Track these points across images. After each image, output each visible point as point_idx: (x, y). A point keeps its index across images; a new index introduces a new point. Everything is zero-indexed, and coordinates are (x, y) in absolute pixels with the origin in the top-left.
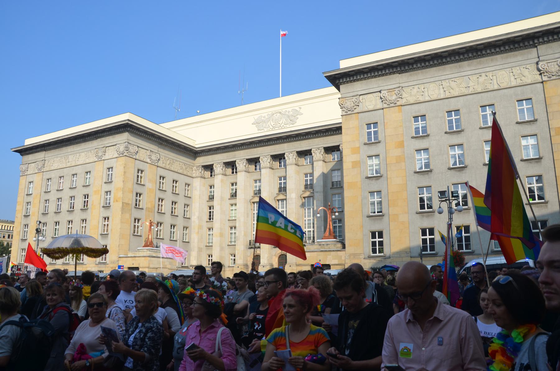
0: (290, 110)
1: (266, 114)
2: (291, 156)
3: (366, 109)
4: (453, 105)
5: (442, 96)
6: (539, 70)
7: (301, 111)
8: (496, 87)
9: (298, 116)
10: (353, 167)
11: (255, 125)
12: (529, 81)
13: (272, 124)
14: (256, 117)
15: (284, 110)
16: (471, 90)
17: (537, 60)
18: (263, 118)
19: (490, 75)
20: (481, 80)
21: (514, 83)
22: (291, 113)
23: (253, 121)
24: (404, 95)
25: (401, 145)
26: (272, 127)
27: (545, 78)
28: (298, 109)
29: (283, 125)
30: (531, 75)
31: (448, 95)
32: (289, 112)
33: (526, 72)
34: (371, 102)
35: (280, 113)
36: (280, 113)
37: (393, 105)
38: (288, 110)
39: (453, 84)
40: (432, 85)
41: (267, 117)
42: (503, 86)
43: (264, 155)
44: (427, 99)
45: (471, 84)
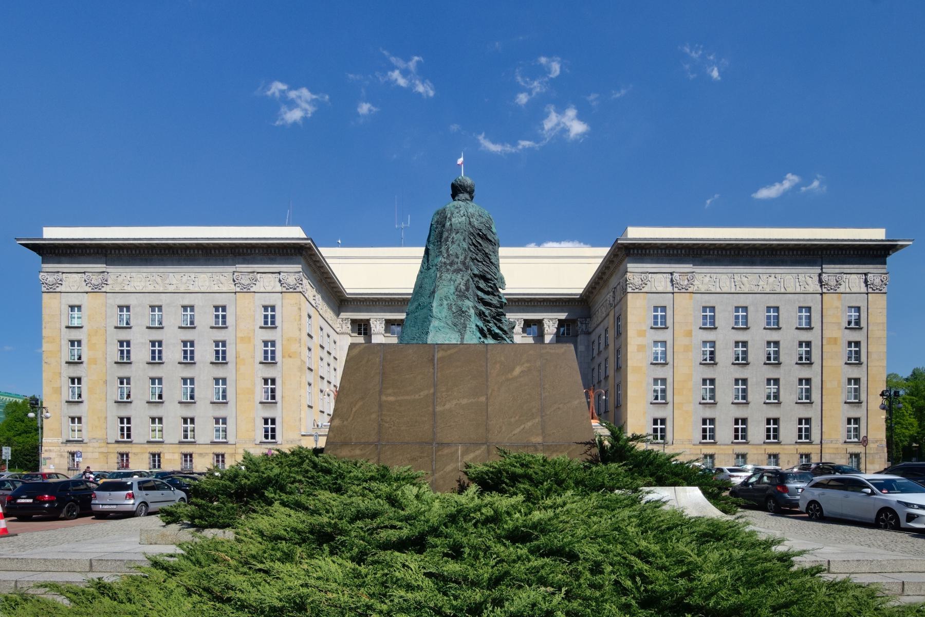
3: (654, 290)
4: (742, 301)
5: (733, 290)
6: (820, 281)
8: (783, 290)
10: (638, 351)
12: (811, 291)
16: (759, 290)
17: (820, 271)
19: (779, 276)
20: (772, 279)
21: (798, 290)
24: (696, 283)
25: (689, 334)
27: (825, 290)
30: (814, 286)
31: (738, 290)
33: (809, 280)
34: (660, 282)
37: (684, 290)
39: (744, 279)
40: (724, 276)
42: (789, 290)
44: (718, 290)
45: (761, 283)
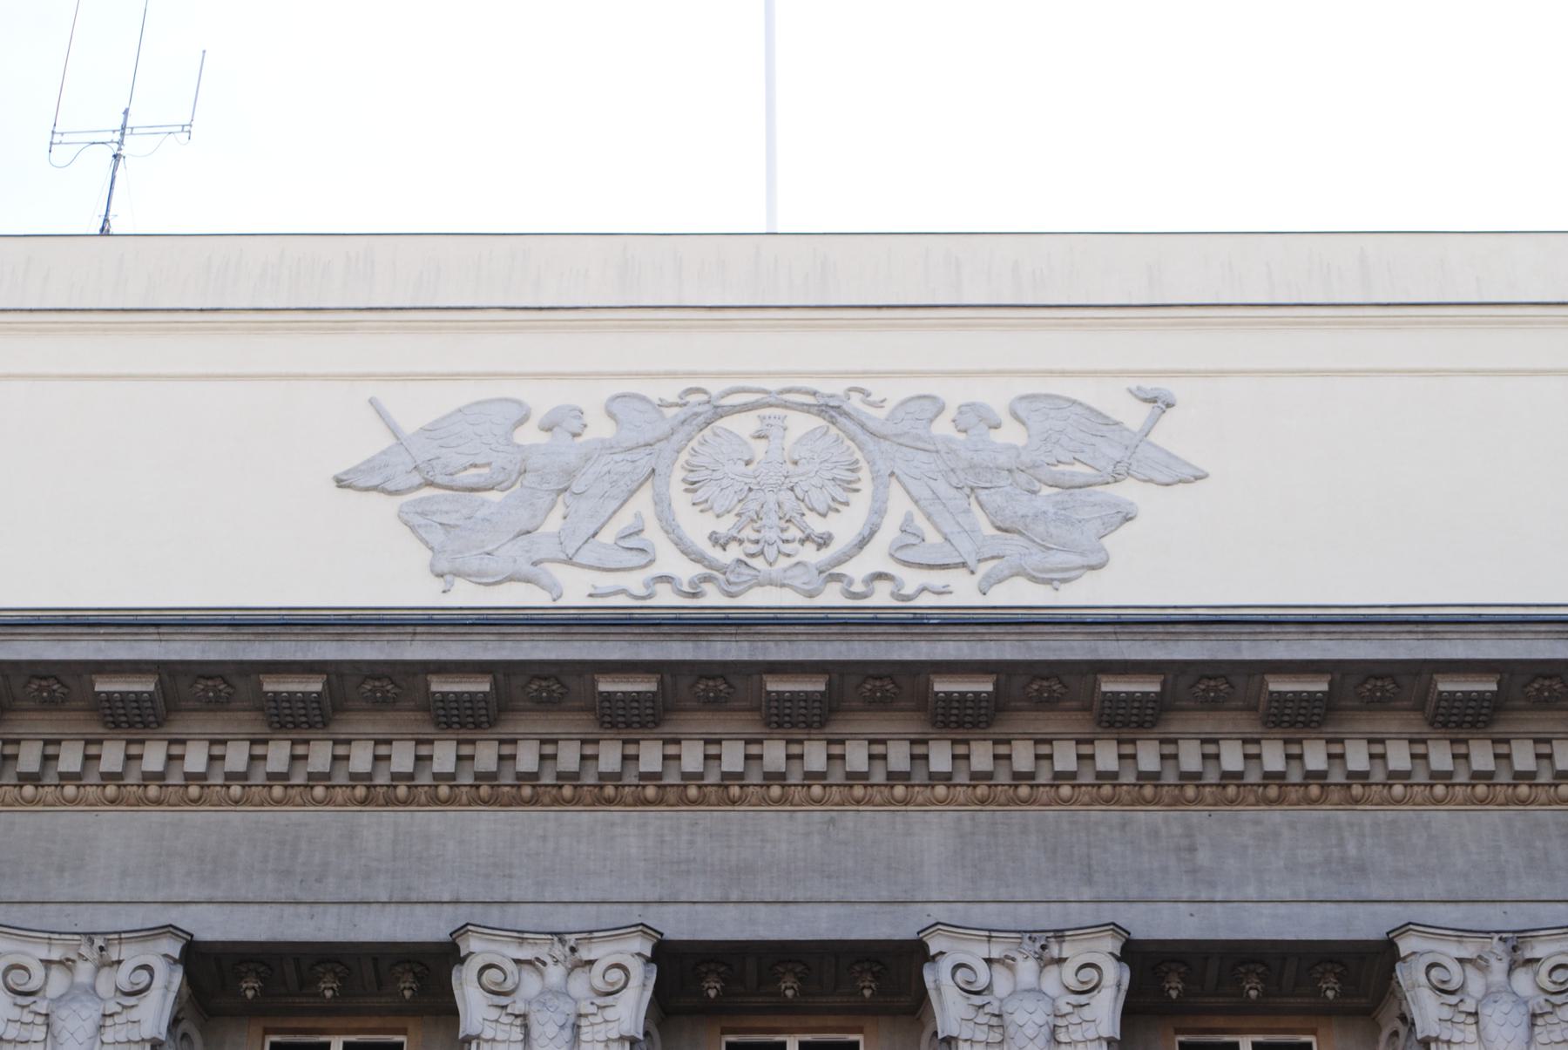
0: (996, 396)
1: (591, 398)
2: (1028, 995)
7: (1171, 435)
9: (1128, 491)
11: (387, 506)
13: (697, 527)
14: (417, 409)
15: (894, 392)
18: (529, 435)
22: (1011, 435)
23: (370, 443)
26: (686, 571)
28: (1134, 415)
29: (874, 559)
32: (977, 418)
35: (830, 411)
36: (830, 411)
38: (955, 394)
41: (600, 429)
43: (527, 918)
